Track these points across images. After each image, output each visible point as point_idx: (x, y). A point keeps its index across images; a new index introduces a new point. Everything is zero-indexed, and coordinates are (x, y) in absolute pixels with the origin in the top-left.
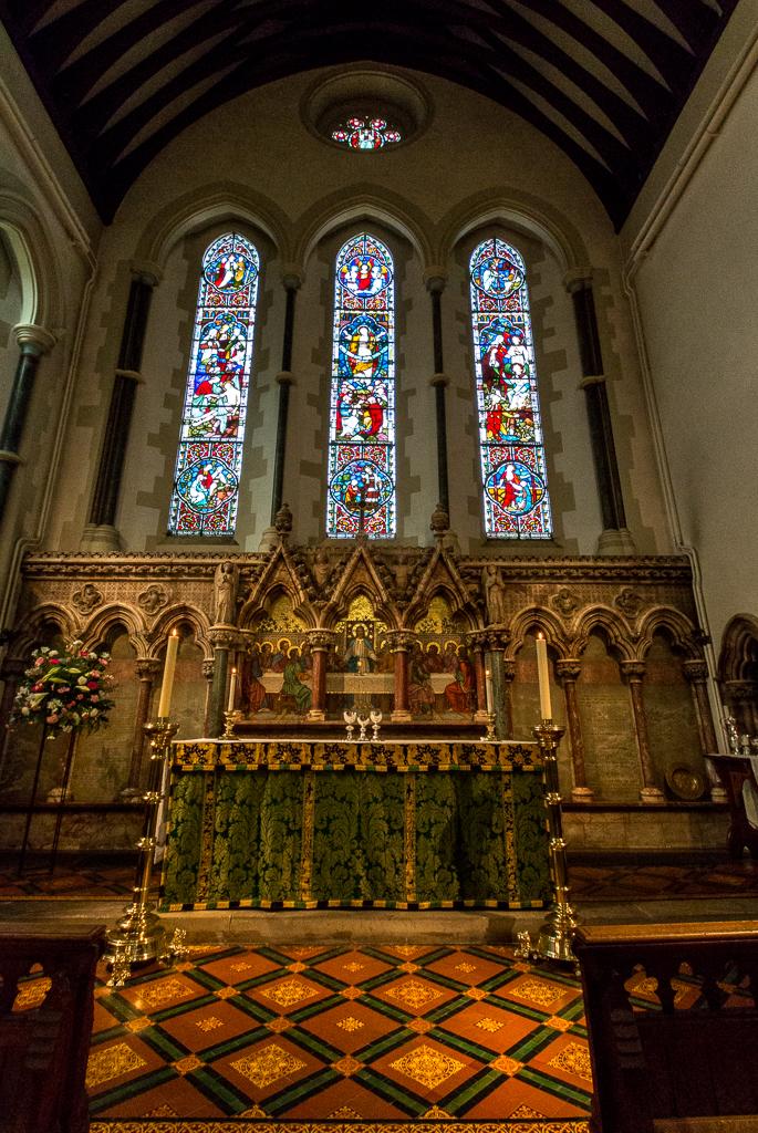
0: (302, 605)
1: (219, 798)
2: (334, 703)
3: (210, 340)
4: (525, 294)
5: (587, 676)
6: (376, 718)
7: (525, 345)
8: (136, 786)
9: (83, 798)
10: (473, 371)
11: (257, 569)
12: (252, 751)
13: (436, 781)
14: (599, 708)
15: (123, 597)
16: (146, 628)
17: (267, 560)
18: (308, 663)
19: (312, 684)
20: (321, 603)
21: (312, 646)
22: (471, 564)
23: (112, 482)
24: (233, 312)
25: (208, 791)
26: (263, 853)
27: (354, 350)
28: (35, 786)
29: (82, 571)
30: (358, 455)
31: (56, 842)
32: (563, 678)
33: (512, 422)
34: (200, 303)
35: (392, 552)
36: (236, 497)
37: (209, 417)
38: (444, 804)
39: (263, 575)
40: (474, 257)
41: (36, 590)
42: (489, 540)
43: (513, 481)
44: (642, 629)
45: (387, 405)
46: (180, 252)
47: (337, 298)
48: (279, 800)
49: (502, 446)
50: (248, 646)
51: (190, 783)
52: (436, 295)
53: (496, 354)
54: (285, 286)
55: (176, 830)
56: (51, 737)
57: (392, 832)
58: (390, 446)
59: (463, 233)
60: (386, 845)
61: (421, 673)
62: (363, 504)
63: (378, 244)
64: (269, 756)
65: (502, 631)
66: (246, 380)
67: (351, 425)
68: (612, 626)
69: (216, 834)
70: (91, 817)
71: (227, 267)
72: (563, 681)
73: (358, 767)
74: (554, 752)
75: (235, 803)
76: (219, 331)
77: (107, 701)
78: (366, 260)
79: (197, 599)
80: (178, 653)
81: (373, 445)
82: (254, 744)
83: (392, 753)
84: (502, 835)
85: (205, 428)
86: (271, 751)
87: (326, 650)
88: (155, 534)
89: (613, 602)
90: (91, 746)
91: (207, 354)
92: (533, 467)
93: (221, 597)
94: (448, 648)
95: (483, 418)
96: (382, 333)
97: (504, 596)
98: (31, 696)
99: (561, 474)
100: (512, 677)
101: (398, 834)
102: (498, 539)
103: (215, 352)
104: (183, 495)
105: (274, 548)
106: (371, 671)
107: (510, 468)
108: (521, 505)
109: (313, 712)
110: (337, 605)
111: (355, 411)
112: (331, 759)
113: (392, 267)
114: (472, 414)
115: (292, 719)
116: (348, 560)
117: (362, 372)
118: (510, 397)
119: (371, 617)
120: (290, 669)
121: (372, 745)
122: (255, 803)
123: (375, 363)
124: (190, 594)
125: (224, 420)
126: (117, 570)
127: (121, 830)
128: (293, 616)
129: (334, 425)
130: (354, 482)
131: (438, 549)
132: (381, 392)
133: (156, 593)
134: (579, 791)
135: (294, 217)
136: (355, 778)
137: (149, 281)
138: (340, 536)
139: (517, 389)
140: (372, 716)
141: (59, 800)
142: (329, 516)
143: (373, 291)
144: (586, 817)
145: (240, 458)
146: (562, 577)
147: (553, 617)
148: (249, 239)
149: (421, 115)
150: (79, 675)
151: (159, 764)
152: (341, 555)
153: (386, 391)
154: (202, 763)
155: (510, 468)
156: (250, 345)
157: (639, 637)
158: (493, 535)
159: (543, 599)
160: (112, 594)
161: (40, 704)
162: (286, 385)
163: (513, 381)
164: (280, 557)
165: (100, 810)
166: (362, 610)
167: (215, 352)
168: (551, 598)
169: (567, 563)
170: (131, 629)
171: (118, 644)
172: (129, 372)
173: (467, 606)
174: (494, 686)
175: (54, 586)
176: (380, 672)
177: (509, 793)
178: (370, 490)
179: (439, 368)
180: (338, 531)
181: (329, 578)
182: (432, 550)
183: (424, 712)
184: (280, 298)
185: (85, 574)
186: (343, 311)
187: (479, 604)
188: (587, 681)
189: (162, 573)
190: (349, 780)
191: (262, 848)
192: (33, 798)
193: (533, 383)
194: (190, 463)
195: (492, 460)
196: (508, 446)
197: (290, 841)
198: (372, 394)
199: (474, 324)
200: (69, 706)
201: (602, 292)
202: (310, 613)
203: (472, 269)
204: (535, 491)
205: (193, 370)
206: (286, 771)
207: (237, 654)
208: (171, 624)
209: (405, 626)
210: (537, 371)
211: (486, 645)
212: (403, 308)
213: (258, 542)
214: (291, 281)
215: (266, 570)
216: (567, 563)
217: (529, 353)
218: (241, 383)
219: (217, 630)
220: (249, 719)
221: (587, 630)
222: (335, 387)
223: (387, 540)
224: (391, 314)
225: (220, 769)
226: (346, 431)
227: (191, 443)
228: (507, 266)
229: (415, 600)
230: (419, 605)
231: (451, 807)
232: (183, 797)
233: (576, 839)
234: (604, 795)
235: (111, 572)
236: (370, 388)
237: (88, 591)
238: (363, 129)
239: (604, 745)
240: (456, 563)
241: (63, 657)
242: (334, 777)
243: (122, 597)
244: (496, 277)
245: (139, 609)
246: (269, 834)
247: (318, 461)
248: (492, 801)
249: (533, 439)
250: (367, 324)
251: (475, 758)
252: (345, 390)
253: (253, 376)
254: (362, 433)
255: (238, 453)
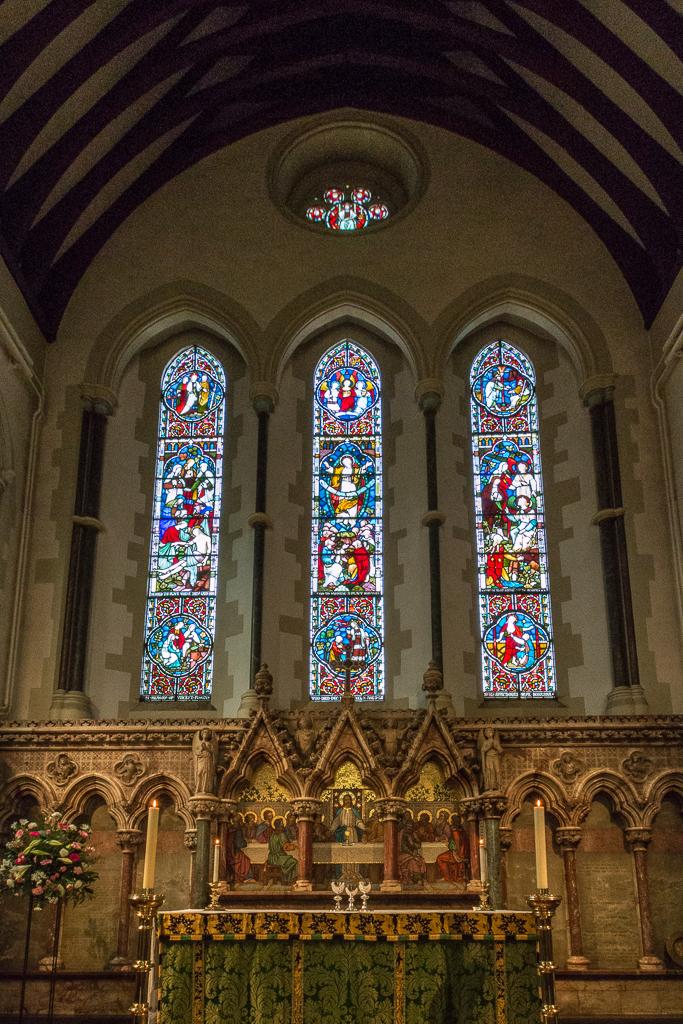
0: (286, 772)
1: (208, 966)
2: (323, 874)
3: (174, 478)
4: (534, 410)
5: (588, 843)
6: (364, 888)
7: (532, 473)
8: (125, 955)
9: (73, 967)
10: (472, 505)
11: (237, 736)
12: (240, 921)
13: (427, 950)
14: (599, 877)
15: (99, 766)
16: (124, 799)
17: (247, 726)
18: (294, 833)
19: (298, 854)
20: (306, 771)
21: (296, 816)
22: (466, 727)
23: (78, 643)
24: (199, 444)
25: (197, 960)
26: (253, 1019)
27: (336, 485)
28: (26, 956)
29: (54, 740)
30: (343, 608)
31: (51, 1007)
32: (561, 846)
33: (515, 566)
34: (161, 434)
35: (380, 716)
36: (212, 658)
37: (177, 568)
38: (434, 972)
39: (244, 742)
40: (475, 365)
41: (9, 761)
42: (487, 700)
43: (515, 634)
44: (651, 794)
45: (374, 550)
46: (135, 369)
47: (316, 422)
48: (268, 968)
49: (504, 594)
50: (231, 816)
51: (179, 953)
52: (430, 414)
53: (498, 485)
54: (254, 407)
55: (168, 996)
56: (38, 909)
57: (381, 999)
58: (378, 597)
59: (462, 336)
60: (376, 1011)
61: (412, 843)
62: (348, 663)
63: (363, 353)
64: (256, 927)
65: (498, 798)
66: (216, 524)
67: (334, 573)
68: (618, 791)
69: (206, 1000)
70: (82, 984)
71: (189, 388)
72: (563, 849)
73: (346, 936)
74: (548, 921)
75: (224, 970)
76: (183, 467)
77: (91, 873)
78: (348, 375)
79: (175, 767)
80: (159, 824)
81: (359, 597)
82: (241, 914)
83: (381, 923)
84: (493, 1002)
85: (174, 581)
86: (258, 921)
87: (311, 819)
88: (127, 700)
89: (620, 767)
90: (78, 916)
91: (172, 495)
92: (537, 617)
93: (200, 765)
94: (441, 816)
95: (482, 562)
96: (369, 464)
97: (501, 761)
98: (14, 868)
99: (569, 624)
100: (508, 846)
101: (388, 1001)
102: (495, 700)
103: (180, 492)
104: (155, 657)
105: (254, 713)
106: (360, 841)
107: (512, 619)
108: (522, 661)
109: (299, 882)
110: (322, 772)
111: (338, 558)
112: (319, 928)
113: (378, 382)
114: (470, 557)
115: (279, 889)
116: (334, 724)
117: (345, 511)
118: (513, 536)
119: (359, 785)
120: (275, 839)
121: (361, 915)
122: (243, 971)
123: (360, 500)
124: (167, 763)
125: (194, 571)
126: (91, 739)
127: (113, 997)
128: (277, 785)
129: (315, 574)
130: (339, 639)
131: (431, 713)
132: (367, 534)
133: (132, 762)
134: (575, 959)
135: (264, 320)
136: (343, 948)
137: (102, 408)
138: (324, 698)
139: (521, 527)
140: (361, 886)
141: (50, 968)
142: (312, 677)
143: (358, 411)
144: (580, 985)
145: (213, 614)
146: (565, 740)
147: (554, 783)
148: (213, 352)
149: (412, 180)
150: (60, 848)
151: (147, 933)
152: (327, 719)
153: (373, 533)
154: (190, 933)
155: (512, 619)
156: (219, 482)
157: (647, 803)
158: (491, 695)
159: (543, 764)
160: (87, 763)
161: (23, 877)
162: (260, 528)
163: (517, 517)
164: (261, 722)
165: (91, 978)
166: (349, 777)
167: (180, 492)
168: (552, 763)
169: (571, 724)
170: (109, 801)
171: (98, 814)
172: (88, 518)
173: (461, 772)
174: (489, 855)
175: (27, 756)
176: (368, 841)
177: (502, 961)
178: (357, 647)
179: (433, 504)
180: (323, 693)
181: (314, 744)
182: (424, 712)
183: (415, 882)
184: (251, 421)
185: (57, 744)
186: (322, 439)
187: (474, 771)
188: (586, 849)
189: (138, 741)
190: (338, 950)
191: (252, 1014)
192: (26, 966)
193: (541, 519)
194: (160, 620)
195: (491, 610)
196: (510, 593)
197: (280, 1007)
198: (357, 537)
199: (474, 449)
200: (53, 878)
201: (625, 405)
202: (295, 782)
203: (472, 380)
204: (538, 645)
205: (158, 514)
206: (274, 941)
207: (219, 824)
208: (150, 794)
209: (395, 794)
210: (546, 505)
211: (480, 813)
212: (392, 430)
213: (237, 706)
214: (263, 404)
215: (246, 736)
216: (571, 724)
217: (536, 483)
218: (211, 527)
219: (198, 800)
220: (234, 890)
221: (590, 796)
222: (316, 529)
223: (375, 703)
224: (378, 440)
225: (207, 938)
226: (329, 580)
227: (159, 598)
228: (514, 376)
229: (405, 766)
230: (409, 771)
231: (441, 975)
232: (172, 966)
233: (569, 1006)
234: (600, 964)
235: (84, 742)
236: (355, 530)
237: (62, 761)
238: (343, 203)
239: (603, 914)
240: (450, 726)
241: (43, 829)
242: (322, 946)
243: (97, 767)
244: (500, 388)
245: (115, 779)
246: (259, 1000)
247: (298, 615)
248: (484, 970)
249: (538, 585)
250: (351, 453)
251: (466, 928)
252: (326, 533)
253: (224, 519)
254: (347, 583)
255: (211, 609)
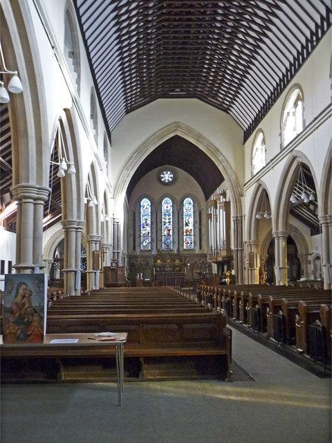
166: (169, 261)
212: (173, 212)
213: (154, 252)
